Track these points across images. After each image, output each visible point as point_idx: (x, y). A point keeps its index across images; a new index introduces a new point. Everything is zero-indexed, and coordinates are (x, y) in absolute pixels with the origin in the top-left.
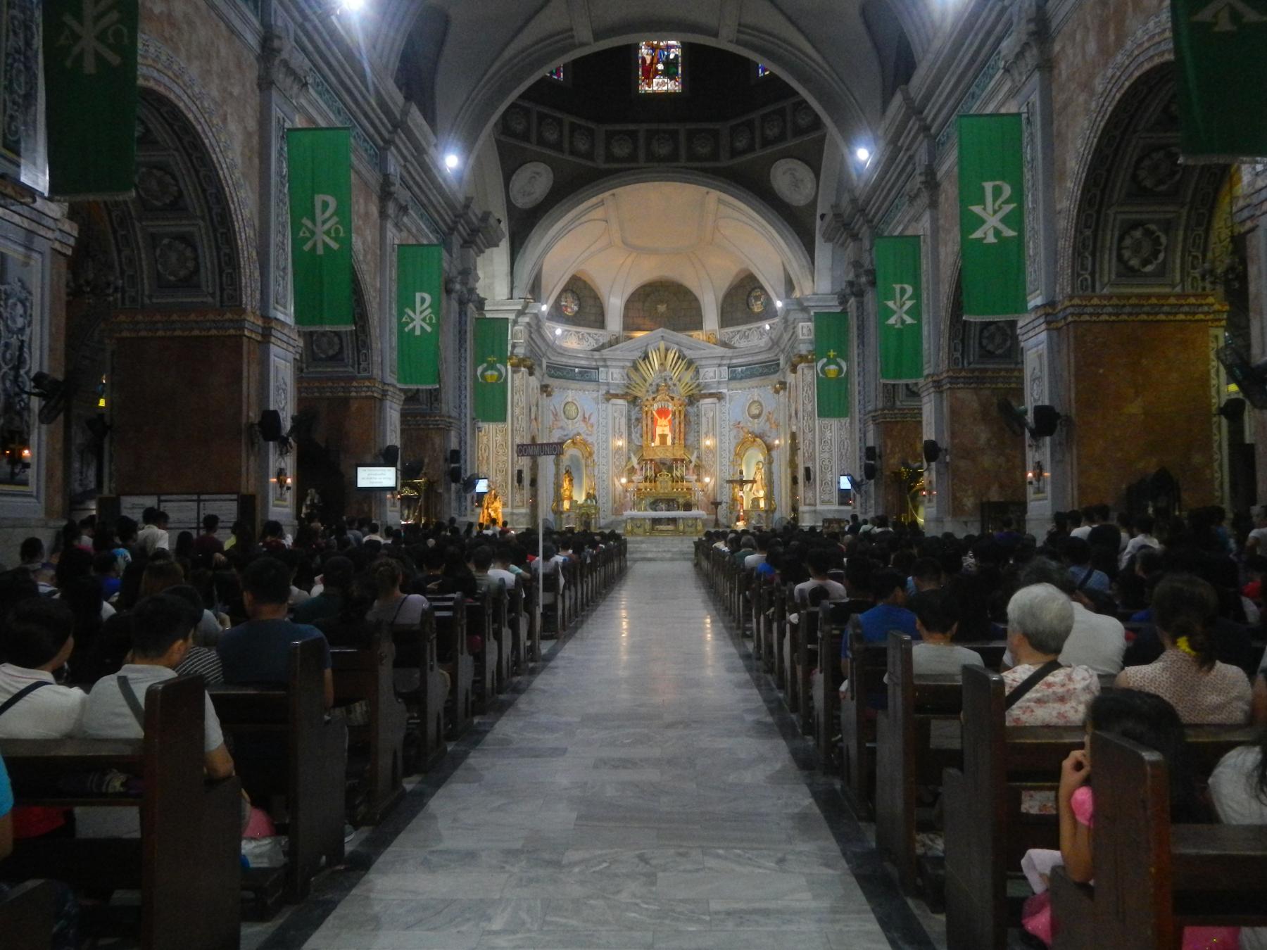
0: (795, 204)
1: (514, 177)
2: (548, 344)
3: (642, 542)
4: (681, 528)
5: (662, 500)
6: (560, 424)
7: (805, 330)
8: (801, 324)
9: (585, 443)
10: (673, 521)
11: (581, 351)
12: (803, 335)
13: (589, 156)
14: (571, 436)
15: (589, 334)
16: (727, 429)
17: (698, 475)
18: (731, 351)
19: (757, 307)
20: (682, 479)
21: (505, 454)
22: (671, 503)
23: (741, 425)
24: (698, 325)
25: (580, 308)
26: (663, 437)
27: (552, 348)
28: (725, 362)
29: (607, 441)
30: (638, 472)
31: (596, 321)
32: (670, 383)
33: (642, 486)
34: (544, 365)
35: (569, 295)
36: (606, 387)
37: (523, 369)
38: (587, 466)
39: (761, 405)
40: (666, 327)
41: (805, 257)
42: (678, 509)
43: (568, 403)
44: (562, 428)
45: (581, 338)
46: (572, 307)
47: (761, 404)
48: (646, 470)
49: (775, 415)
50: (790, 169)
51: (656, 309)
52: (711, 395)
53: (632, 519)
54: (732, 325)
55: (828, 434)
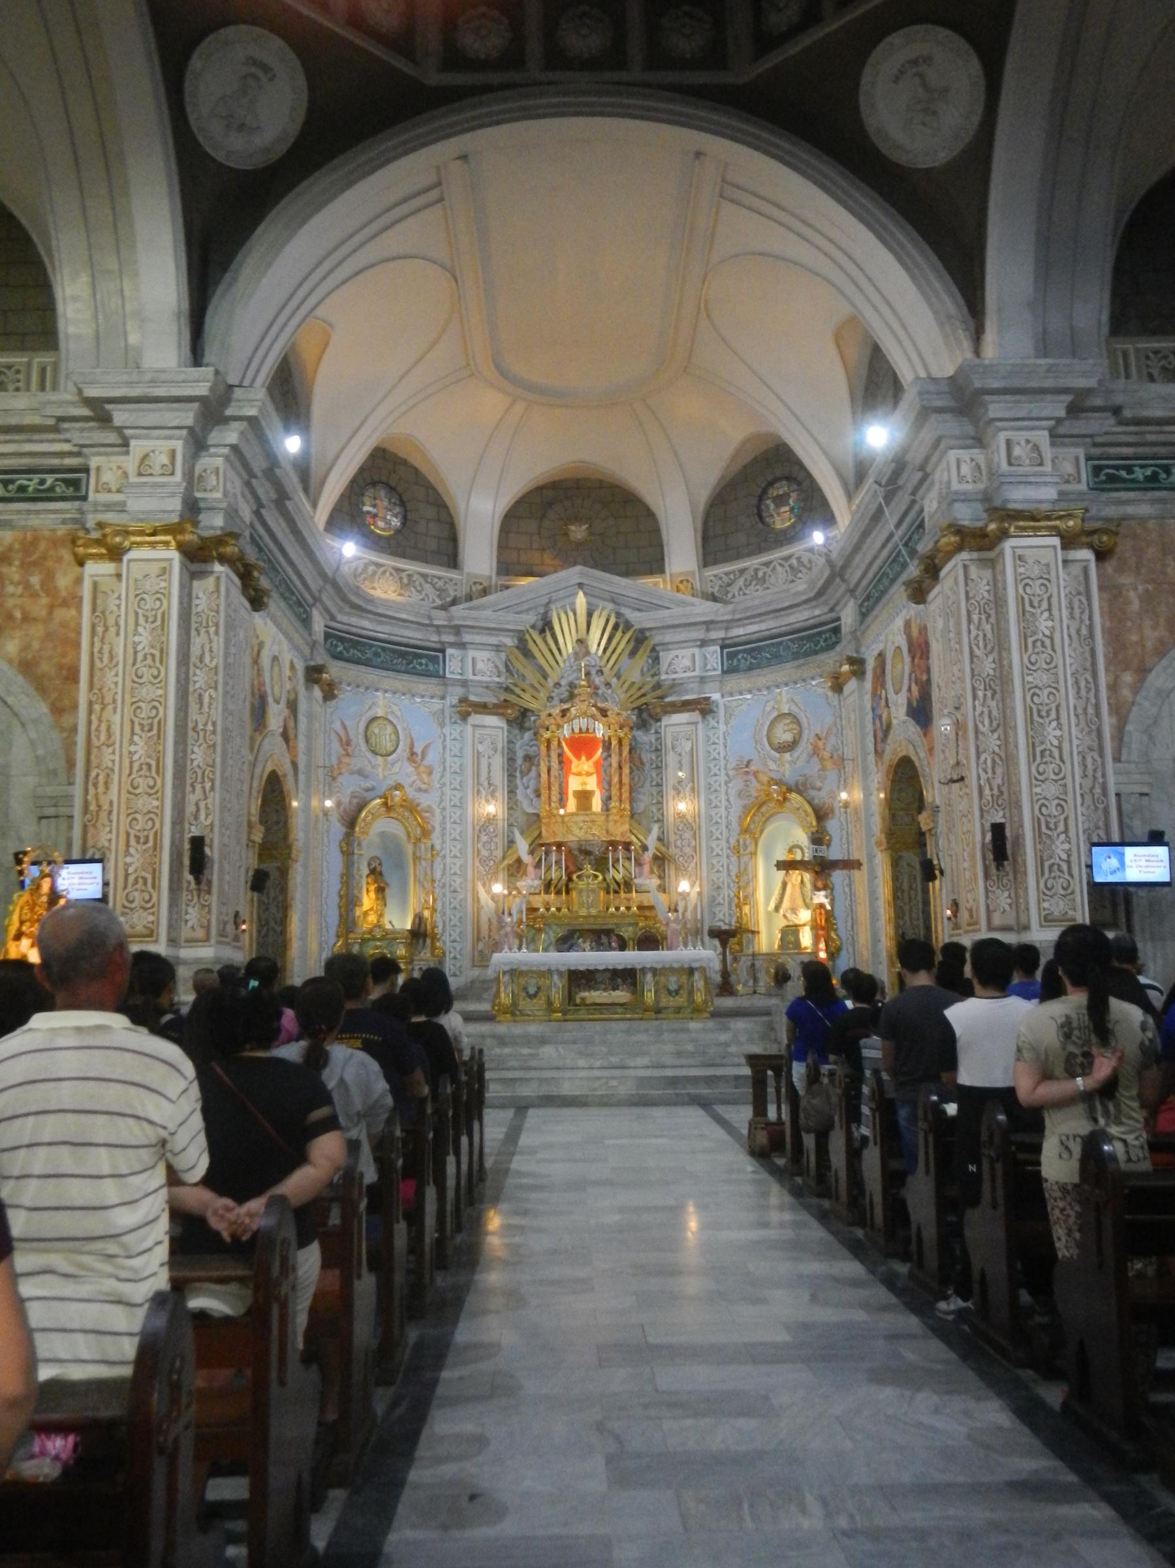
0: (922, 163)
1: (195, 63)
2: (322, 574)
3: (543, 1041)
4: (649, 997)
5: (583, 933)
6: (357, 763)
7: (966, 469)
8: (953, 455)
9: (411, 807)
10: (627, 977)
11: (400, 607)
12: (961, 479)
14: (383, 789)
15: (424, 576)
16: (723, 778)
17: (660, 877)
18: (730, 607)
19: (782, 520)
20: (628, 885)
21: (154, 791)
22: (602, 937)
23: (753, 768)
24: (655, 564)
26: (584, 797)
27: (335, 585)
28: (714, 635)
29: (461, 805)
30: (530, 869)
32: (598, 680)
33: (538, 901)
34: (319, 624)
35: (382, 493)
36: (459, 691)
37: (218, 567)
38: (417, 859)
39: (799, 723)
40: (585, 564)
41: (952, 296)
42: (623, 946)
43: (374, 719)
44: (360, 772)
45: (406, 583)
46: (388, 521)
47: (796, 720)
48: (549, 868)
49: (832, 740)
50: (914, 62)
51: (566, 534)
52: (686, 706)
53: (515, 973)
54: (726, 560)
55: (1052, 733)
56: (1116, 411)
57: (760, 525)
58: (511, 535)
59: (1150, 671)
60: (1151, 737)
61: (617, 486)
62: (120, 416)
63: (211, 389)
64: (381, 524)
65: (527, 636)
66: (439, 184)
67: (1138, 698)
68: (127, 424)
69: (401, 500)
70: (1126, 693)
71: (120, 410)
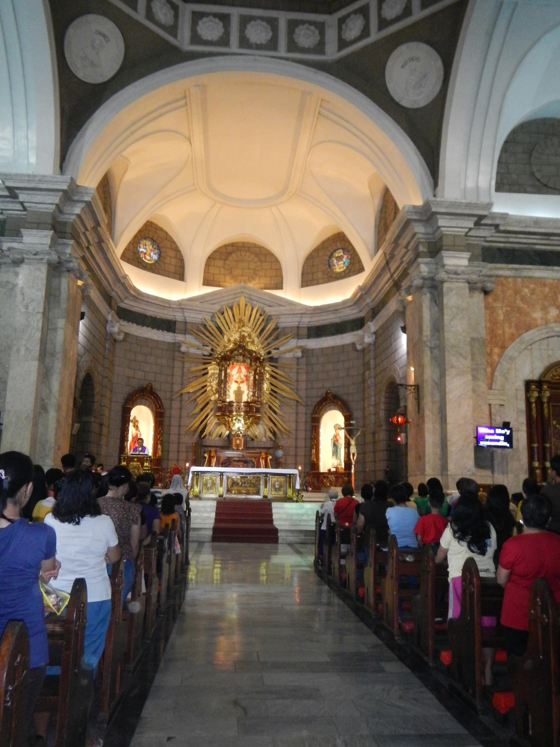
13: (173, 30)
19: (339, 267)
25: (159, 258)
31: (175, 273)
56: (496, 226)
57: (329, 269)
58: (210, 267)
59: (507, 348)
60: (506, 379)
61: (263, 248)
62: (23, 197)
63: (69, 187)
64: (148, 257)
65: (216, 315)
66: (185, 97)
67: (501, 360)
68: (26, 201)
69: (158, 246)
70: (496, 357)
71: (22, 193)
